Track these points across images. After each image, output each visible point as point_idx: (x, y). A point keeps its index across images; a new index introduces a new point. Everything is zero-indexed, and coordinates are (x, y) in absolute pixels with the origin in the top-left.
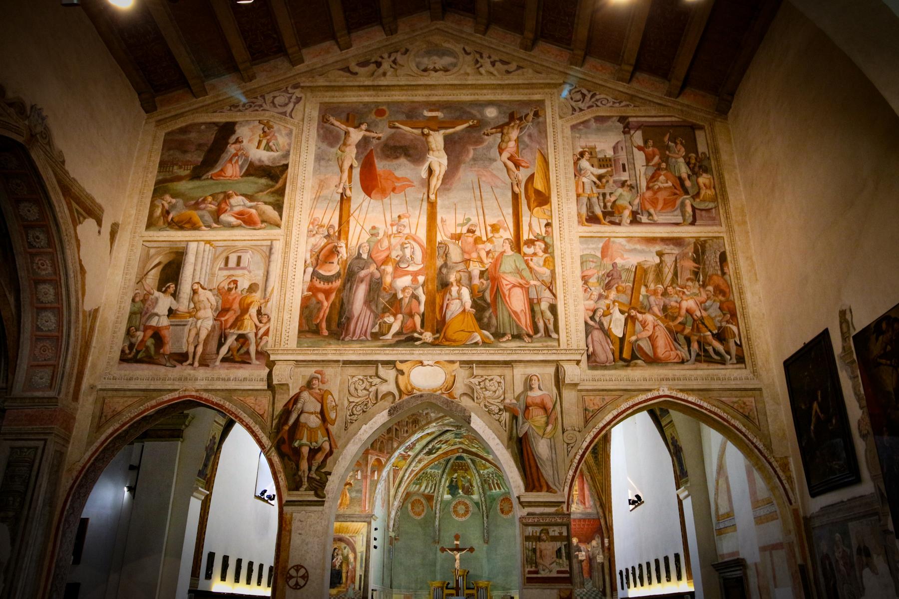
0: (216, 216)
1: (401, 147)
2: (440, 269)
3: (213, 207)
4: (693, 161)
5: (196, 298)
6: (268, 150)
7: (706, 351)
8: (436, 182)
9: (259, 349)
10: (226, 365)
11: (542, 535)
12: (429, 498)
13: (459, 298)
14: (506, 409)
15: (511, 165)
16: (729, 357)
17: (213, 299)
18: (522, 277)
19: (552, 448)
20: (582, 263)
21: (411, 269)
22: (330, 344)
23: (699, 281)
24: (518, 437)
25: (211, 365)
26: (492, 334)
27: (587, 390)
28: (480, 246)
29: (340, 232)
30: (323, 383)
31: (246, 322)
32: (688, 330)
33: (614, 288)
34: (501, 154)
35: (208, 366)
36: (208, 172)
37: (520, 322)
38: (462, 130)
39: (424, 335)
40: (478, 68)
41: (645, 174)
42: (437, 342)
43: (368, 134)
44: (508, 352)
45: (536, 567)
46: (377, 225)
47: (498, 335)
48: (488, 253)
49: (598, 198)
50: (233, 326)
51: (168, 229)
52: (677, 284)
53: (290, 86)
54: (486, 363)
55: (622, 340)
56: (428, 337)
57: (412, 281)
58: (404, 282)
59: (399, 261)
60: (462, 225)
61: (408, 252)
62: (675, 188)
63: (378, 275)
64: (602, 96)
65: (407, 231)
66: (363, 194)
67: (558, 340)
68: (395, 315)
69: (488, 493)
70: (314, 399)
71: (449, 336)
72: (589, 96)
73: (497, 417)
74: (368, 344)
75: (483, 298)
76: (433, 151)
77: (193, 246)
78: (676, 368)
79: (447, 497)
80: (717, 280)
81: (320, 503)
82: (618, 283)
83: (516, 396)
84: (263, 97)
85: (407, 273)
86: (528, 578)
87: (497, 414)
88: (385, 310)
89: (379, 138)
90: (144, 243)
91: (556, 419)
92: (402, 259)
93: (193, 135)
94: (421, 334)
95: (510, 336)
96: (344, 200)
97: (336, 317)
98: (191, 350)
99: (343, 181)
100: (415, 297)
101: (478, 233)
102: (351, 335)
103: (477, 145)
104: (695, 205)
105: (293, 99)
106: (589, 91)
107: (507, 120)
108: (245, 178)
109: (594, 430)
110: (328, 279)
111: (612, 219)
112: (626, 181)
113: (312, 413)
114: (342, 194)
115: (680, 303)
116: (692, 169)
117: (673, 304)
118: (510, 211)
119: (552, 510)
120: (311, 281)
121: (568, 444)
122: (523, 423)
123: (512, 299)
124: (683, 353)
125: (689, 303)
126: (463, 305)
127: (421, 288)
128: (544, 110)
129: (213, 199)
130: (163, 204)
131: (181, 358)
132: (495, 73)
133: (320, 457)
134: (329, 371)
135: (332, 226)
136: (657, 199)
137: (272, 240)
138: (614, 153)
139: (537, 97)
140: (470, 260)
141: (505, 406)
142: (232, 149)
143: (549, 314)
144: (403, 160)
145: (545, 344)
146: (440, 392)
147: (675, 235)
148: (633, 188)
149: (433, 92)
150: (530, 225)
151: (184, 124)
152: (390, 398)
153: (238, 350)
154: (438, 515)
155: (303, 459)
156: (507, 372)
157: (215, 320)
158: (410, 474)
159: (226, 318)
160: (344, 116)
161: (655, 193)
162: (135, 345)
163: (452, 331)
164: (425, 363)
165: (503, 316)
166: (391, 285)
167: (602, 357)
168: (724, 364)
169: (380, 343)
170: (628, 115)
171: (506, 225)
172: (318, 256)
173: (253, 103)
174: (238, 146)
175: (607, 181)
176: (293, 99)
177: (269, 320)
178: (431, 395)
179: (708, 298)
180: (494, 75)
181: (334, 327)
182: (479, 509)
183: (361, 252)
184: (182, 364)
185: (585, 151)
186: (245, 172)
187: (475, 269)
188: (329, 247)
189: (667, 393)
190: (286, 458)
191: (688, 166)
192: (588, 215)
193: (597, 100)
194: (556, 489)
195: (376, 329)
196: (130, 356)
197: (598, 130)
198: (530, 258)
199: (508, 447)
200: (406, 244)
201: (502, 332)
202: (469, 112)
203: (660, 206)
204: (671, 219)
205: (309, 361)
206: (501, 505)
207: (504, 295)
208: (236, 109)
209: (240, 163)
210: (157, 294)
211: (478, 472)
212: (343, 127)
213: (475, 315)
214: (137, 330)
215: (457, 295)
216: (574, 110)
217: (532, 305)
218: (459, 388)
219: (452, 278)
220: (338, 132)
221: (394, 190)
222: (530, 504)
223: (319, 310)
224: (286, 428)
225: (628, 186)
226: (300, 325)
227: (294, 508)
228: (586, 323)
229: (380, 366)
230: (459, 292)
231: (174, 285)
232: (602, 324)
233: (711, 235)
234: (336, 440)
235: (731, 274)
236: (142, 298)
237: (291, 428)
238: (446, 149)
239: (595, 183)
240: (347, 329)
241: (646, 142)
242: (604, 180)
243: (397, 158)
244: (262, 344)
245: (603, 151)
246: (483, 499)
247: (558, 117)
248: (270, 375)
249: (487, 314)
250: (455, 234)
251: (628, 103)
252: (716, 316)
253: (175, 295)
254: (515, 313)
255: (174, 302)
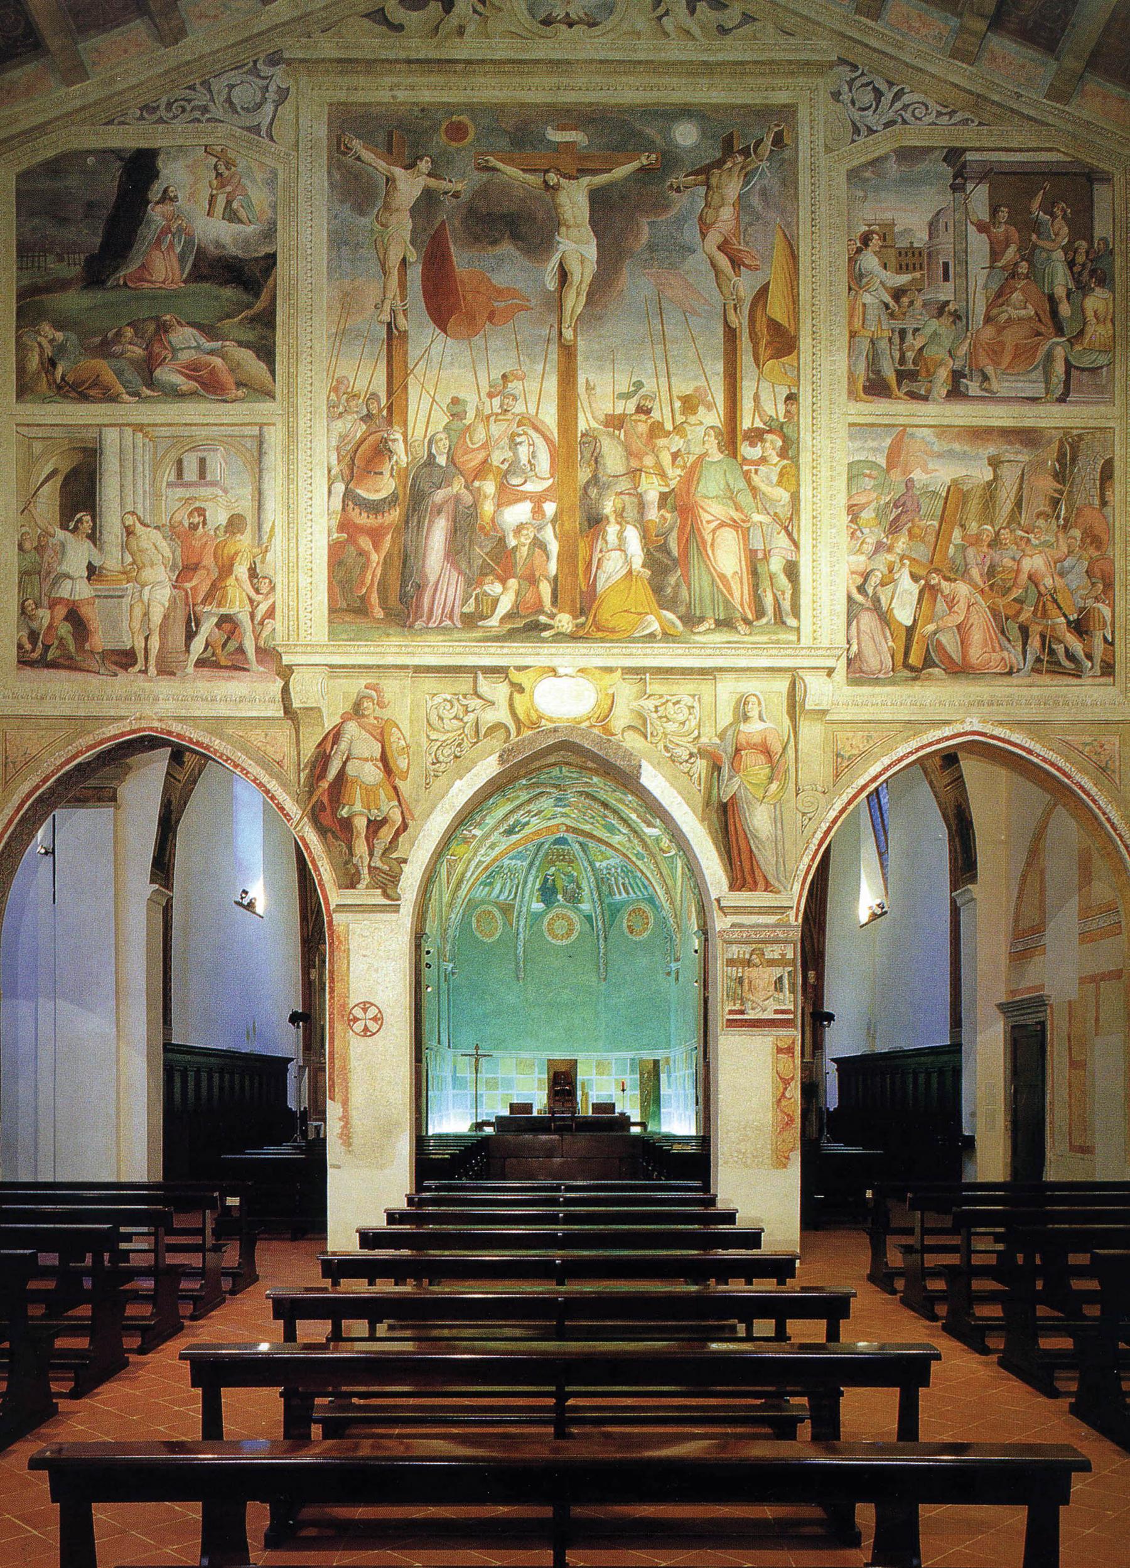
0: (147, 368)
1: (503, 217)
2: (585, 489)
3: (138, 352)
4: (1081, 259)
5: (133, 543)
6: (230, 221)
7: (1052, 652)
8: (574, 301)
9: (262, 643)
10: (206, 672)
11: (754, 957)
12: (506, 909)
13: (621, 548)
14: (702, 753)
15: (723, 262)
16: (1090, 664)
17: (164, 546)
18: (738, 508)
19: (778, 821)
20: (850, 479)
21: (529, 487)
22: (388, 635)
23: (1058, 518)
24: (720, 802)
25: (179, 674)
26: (680, 618)
27: (842, 722)
28: (661, 442)
29: (390, 409)
30: (381, 705)
31: (230, 590)
32: (1026, 615)
33: (905, 531)
34: (704, 235)
35: (173, 674)
36: (116, 269)
37: (731, 595)
38: (627, 179)
39: (558, 618)
40: (660, 18)
41: (985, 287)
42: (581, 633)
43: (433, 183)
44: (709, 652)
45: (742, 1004)
46: (461, 396)
47: (691, 620)
48: (675, 456)
49: (890, 339)
50: (208, 599)
51: (58, 398)
52: (1019, 524)
53: (262, 56)
54: (670, 671)
55: (910, 631)
56: (564, 623)
57: (534, 512)
58: (517, 514)
59: (507, 472)
60: (627, 396)
61: (523, 452)
62: (1040, 321)
63: (468, 499)
64: (916, 97)
65: (519, 408)
66: (433, 326)
67: (798, 629)
68: (503, 581)
69: (607, 901)
70: (368, 736)
71: (603, 622)
72: (890, 96)
73: (685, 767)
74: (456, 636)
75: (664, 549)
76: (568, 227)
77: (111, 437)
78: (997, 683)
79: (538, 906)
80: (1091, 517)
81: (393, 909)
82: (912, 520)
83: (719, 731)
84: (206, 84)
85: (523, 497)
86: (728, 1020)
87: (687, 761)
88: (485, 571)
89: (456, 195)
90: (19, 429)
91: (787, 771)
92: (514, 467)
93: (73, 181)
94: (552, 616)
95: (712, 621)
96: (395, 338)
97: (395, 584)
98: (140, 645)
99: (390, 295)
100: (539, 544)
101: (656, 415)
102: (425, 619)
103: (657, 215)
104: (1071, 358)
105: (271, 95)
106: (891, 84)
107: (718, 155)
108: (193, 286)
109: (849, 790)
110: (374, 508)
111: (914, 386)
112: (947, 303)
113: (366, 760)
114: (389, 324)
115: (1019, 562)
116: (1076, 278)
117: (1008, 562)
118: (720, 367)
119: (771, 919)
120: (343, 509)
121: (804, 814)
122: (731, 778)
123: (718, 552)
124: (1013, 655)
125: (1034, 563)
126: (627, 561)
127: (550, 525)
128: (794, 128)
129: (136, 334)
130: (40, 344)
131: (125, 659)
132: (696, 31)
133: (387, 834)
134: (391, 687)
135: (374, 396)
136: (1002, 344)
137: (261, 426)
138: (930, 238)
139: (781, 98)
140: (641, 470)
141: (699, 749)
142: (157, 214)
143: (783, 581)
144: (506, 248)
145: (774, 637)
146: (587, 724)
147: (1028, 423)
148: (959, 318)
149: (566, 81)
150: (756, 398)
151: (51, 154)
152: (501, 734)
153: (224, 645)
154: (521, 936)
155: (357, 837)
156: (705, 688)
157: (175, 587)
158: (477, 867)
159: (194, 583)
160: (381, 137)
161: (1000, 330)
162: (39, 634)
163: (609, 610)
164: (561, 671)
165: (700, 581)
166: (493, 520)
167: (872, 662)
168: (1079, 677)
169: (478, 634)
170: (965, 145)
171: (710, 398)
172: (353, 459)
173: (189, 101)
174: (167, 208)
175: (911, 303)
176: (271, 95)
177: (273, 589)
178: (573, 729)
179: (1070, 552)
180: (694, 39)
181: (393, 601)
182: (592, 926)
183: (434, 451)
184: (126, 670)
185: (872, 232)
186: (190, 274)
187: (651, 489)
188: (372, 439)
189: (978, 727)
190: (329, 834)
191: (1071, 269)
192: (868, 379)
193: (905, 107)
194: (781, 888)
195: (470, 608)
196: (35, 655)
197: (904, 180)
198: (753, 468)
199: (703, 820)
200: (520, 435)
201: (698, 614)
202: (641, 134)
203: (1006, 360)
204: (1023, 390)
205: (353, 667)
206: (629, 921)
207: (704, 542)
208: (155, 117)
209: (178, 250)
210: (61, 534)
211: (591, 864)
212: (381, 165)
213: (650, 581)
214: (38, 605)
215: (616, 542)
216: (857, 131)
217: (754, 563)
218: (621, 719)
219: (608, 507)
220: (371, 178)
221: (491, 317)
222: (737, 910)
223: (365, 567)
224: (325, 785)
225: (950, 314)
226: (331, 598)
227: (350, 916)
228: (850, 598)
229: (480, 675)
230: (620, 536)
231: (89, 518)
232: (879, 601)
233: (1092, 423)
234: (412, 807)
235: (1117, 505)
236: (35, 544)
237: (332, 785)
238: (593, 223)
239: (887, 306)
240: (419, 606)
241: (994, 211)
242: (905, 300)
243: (494, 242)
244: (264, 635)
245: (908, 231)
246: (599, 910)
247: (822, 149)
248: (285, 691)
249: (672, 580)
250: (613, 416)
251: (968, 115)
252: (1078, 588)
253: (93, 537)
254: (723, 577)
255: (95, 551)
